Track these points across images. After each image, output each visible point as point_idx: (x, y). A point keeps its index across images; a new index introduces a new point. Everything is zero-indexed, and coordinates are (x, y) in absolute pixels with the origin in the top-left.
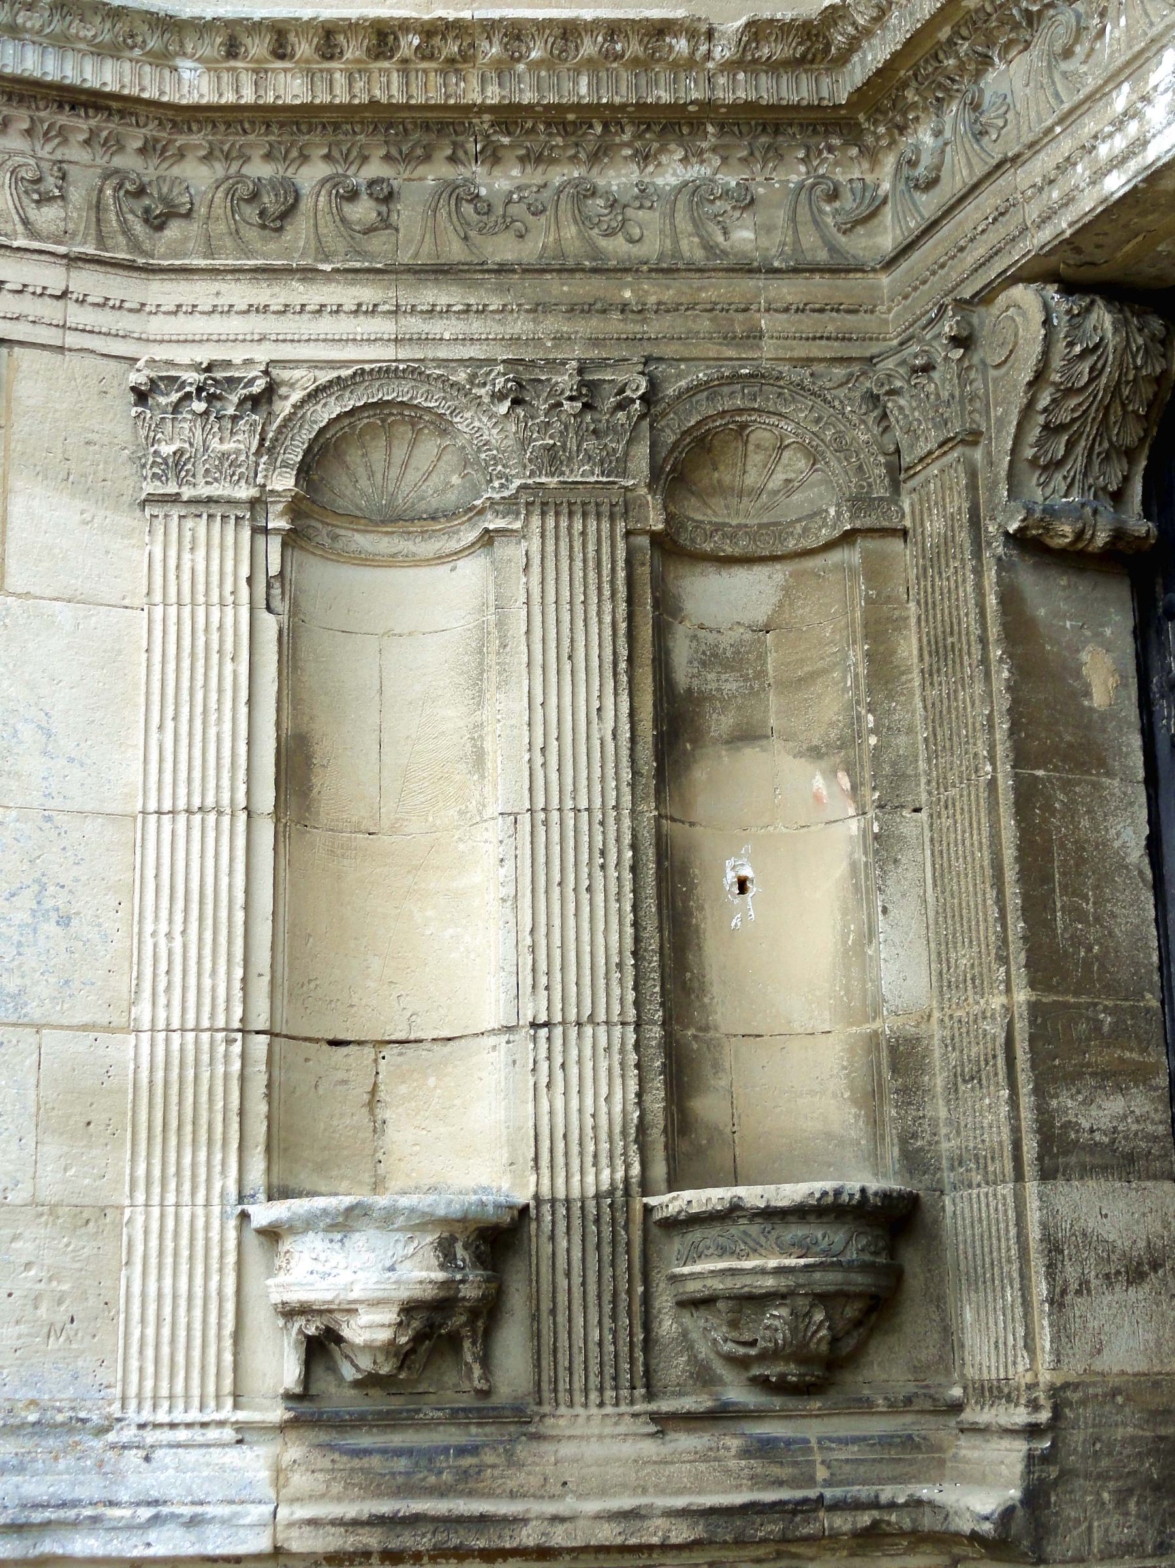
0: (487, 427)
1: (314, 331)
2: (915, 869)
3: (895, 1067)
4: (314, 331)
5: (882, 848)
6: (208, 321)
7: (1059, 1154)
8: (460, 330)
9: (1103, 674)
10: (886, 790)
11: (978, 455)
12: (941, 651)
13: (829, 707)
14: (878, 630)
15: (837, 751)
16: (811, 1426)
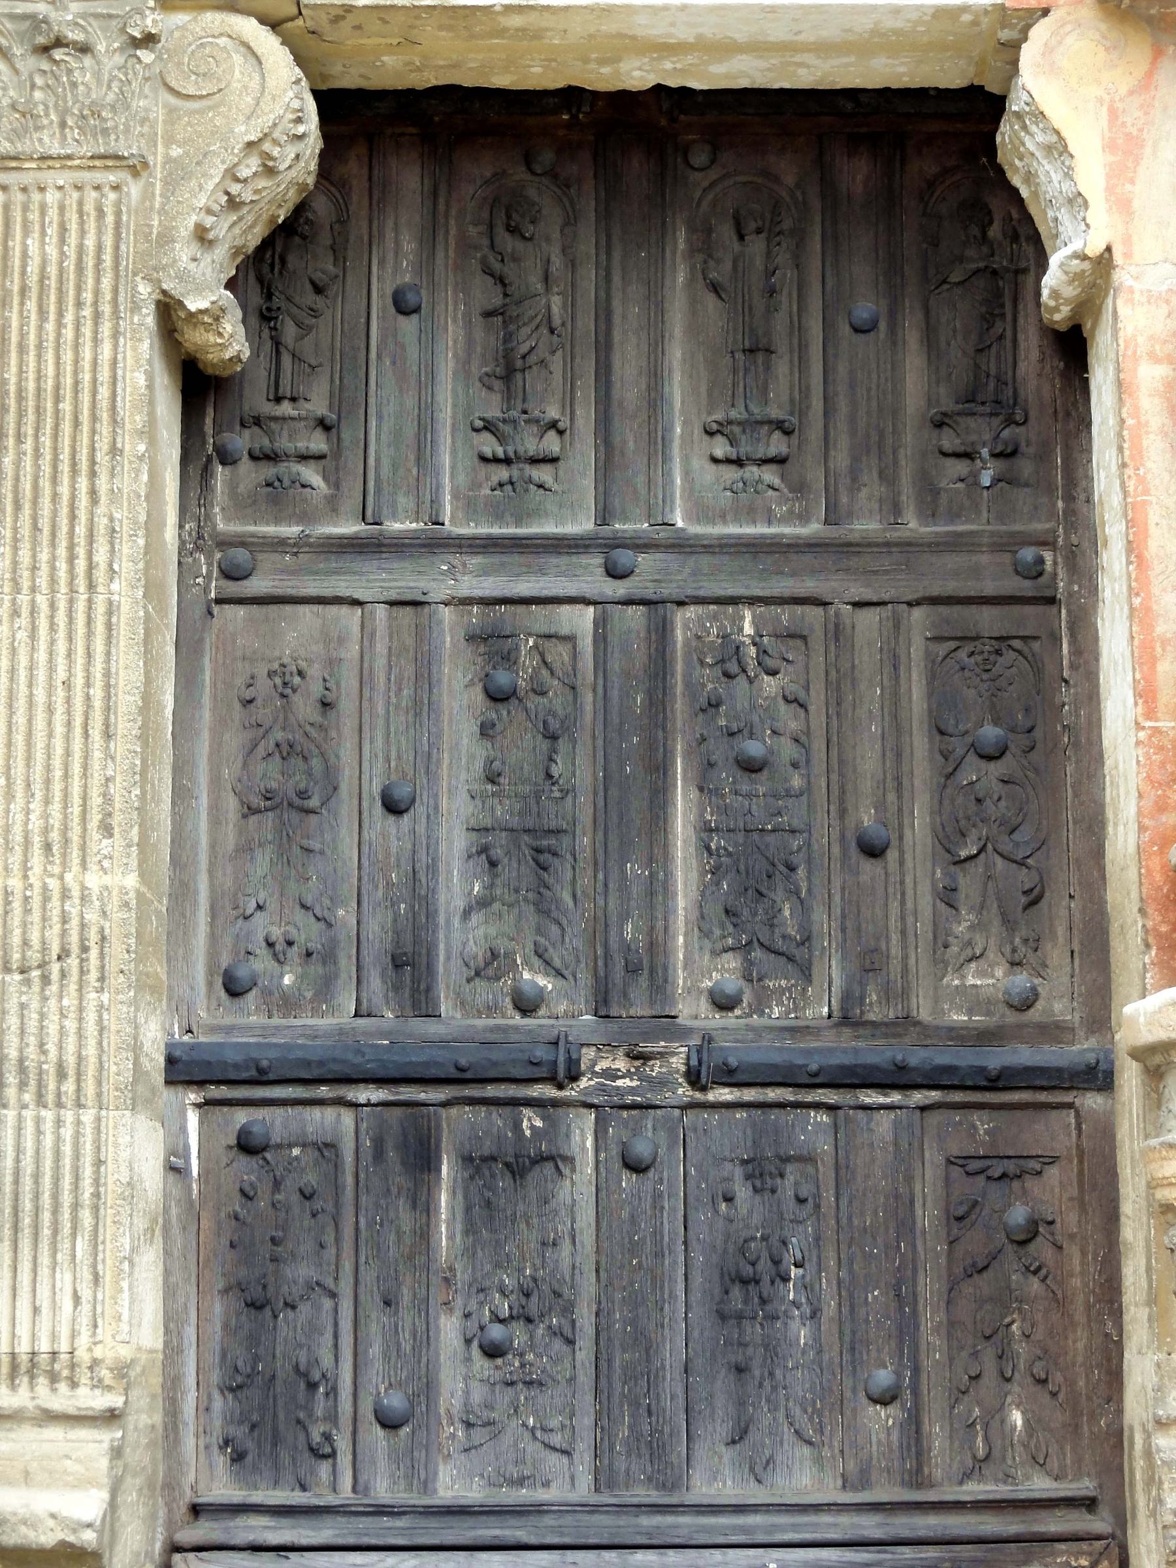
11: (134, 189)
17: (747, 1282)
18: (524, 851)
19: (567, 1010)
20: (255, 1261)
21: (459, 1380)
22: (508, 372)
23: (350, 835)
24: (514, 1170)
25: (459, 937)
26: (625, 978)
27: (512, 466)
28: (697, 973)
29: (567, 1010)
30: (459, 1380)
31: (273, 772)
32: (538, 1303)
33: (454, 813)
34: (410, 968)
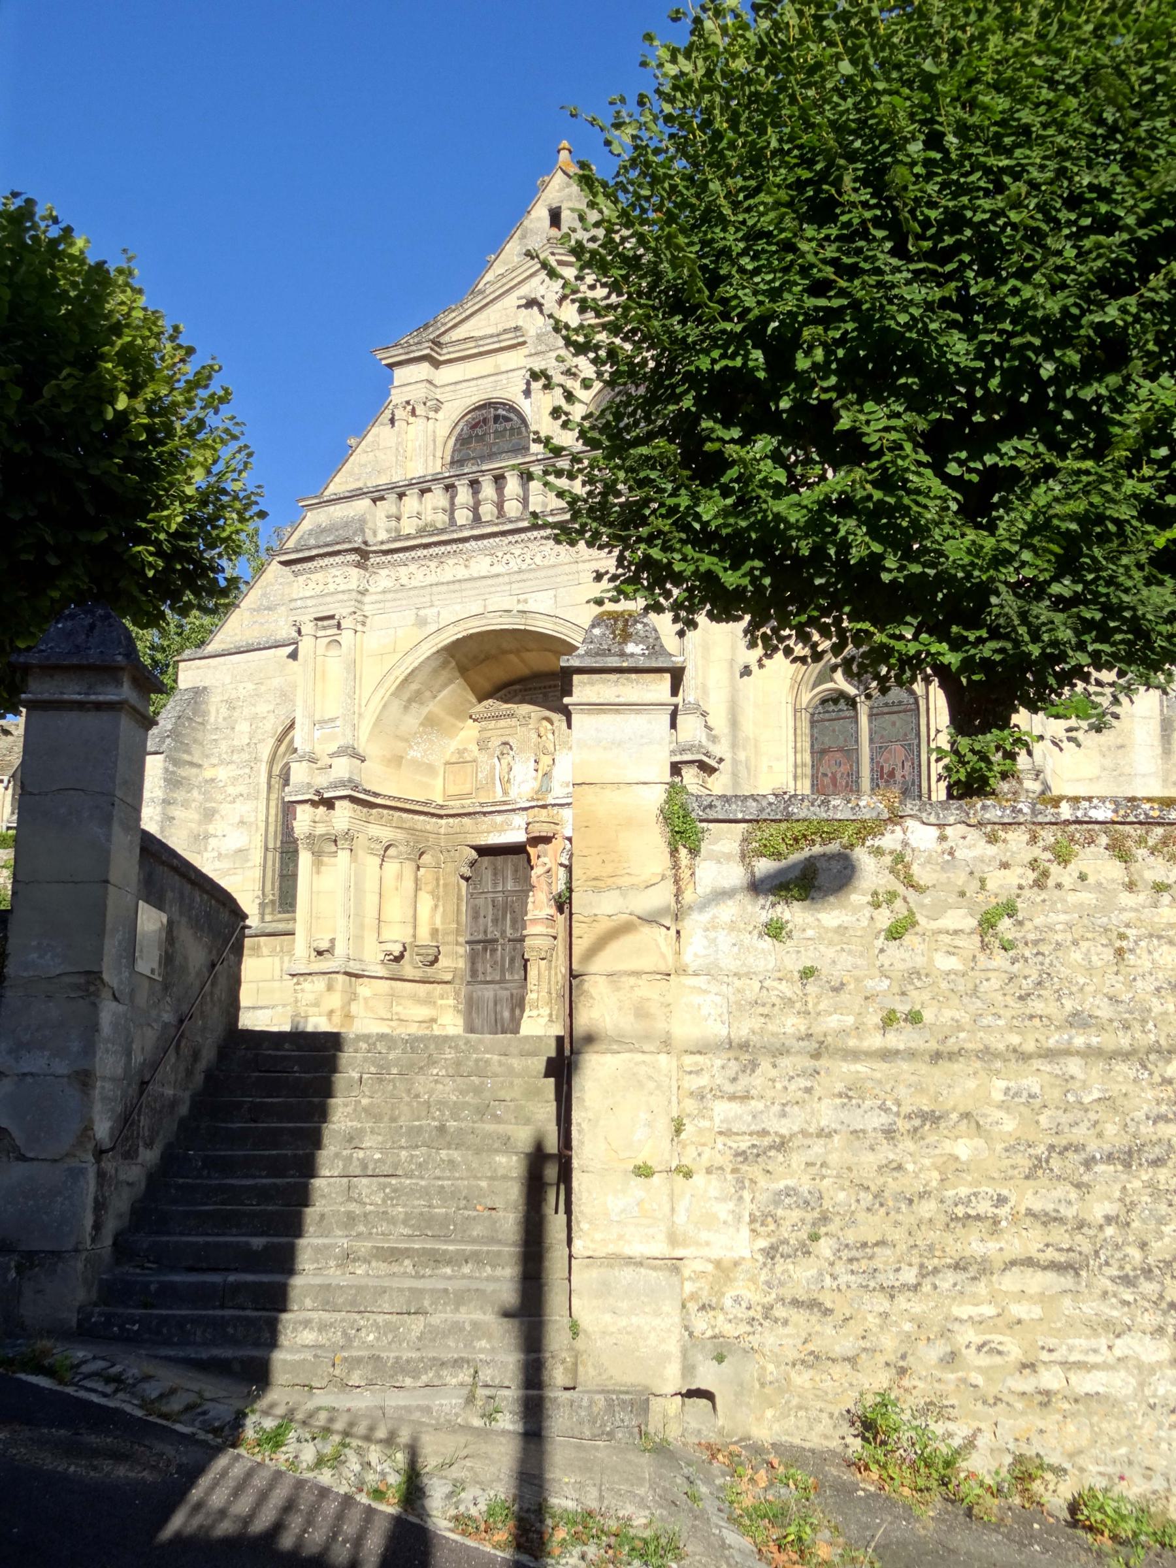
0: (402, 849)
1: (386, 833)
2: (441, 909)
3: (434, 932)
4: (386, 833)
5: (436, 906)
6: (375, 830)
7: (457, 944)
8: (400, 835)
9: (464, 892)
10: (437, 898)
12: (445, 885)
13: (430, 888)
14: (437, 880)
15: (432, 893)
16: (428, 969)
17: (512, 960)
18: (495, 921)
19: (498, 935)
20: (473, 958)
21: (489, 970)
22: (495, 874)
23: (481, 920)
24: (494, 951)
25: (490, 929)
26: (503, 932)
27: (495, 884)
28: (509, 932)
29: (498, 935)
30: (489, 970)
31: (475, 915)
32: (496, 963)
33: (490, 918)
34: (485, 932)
